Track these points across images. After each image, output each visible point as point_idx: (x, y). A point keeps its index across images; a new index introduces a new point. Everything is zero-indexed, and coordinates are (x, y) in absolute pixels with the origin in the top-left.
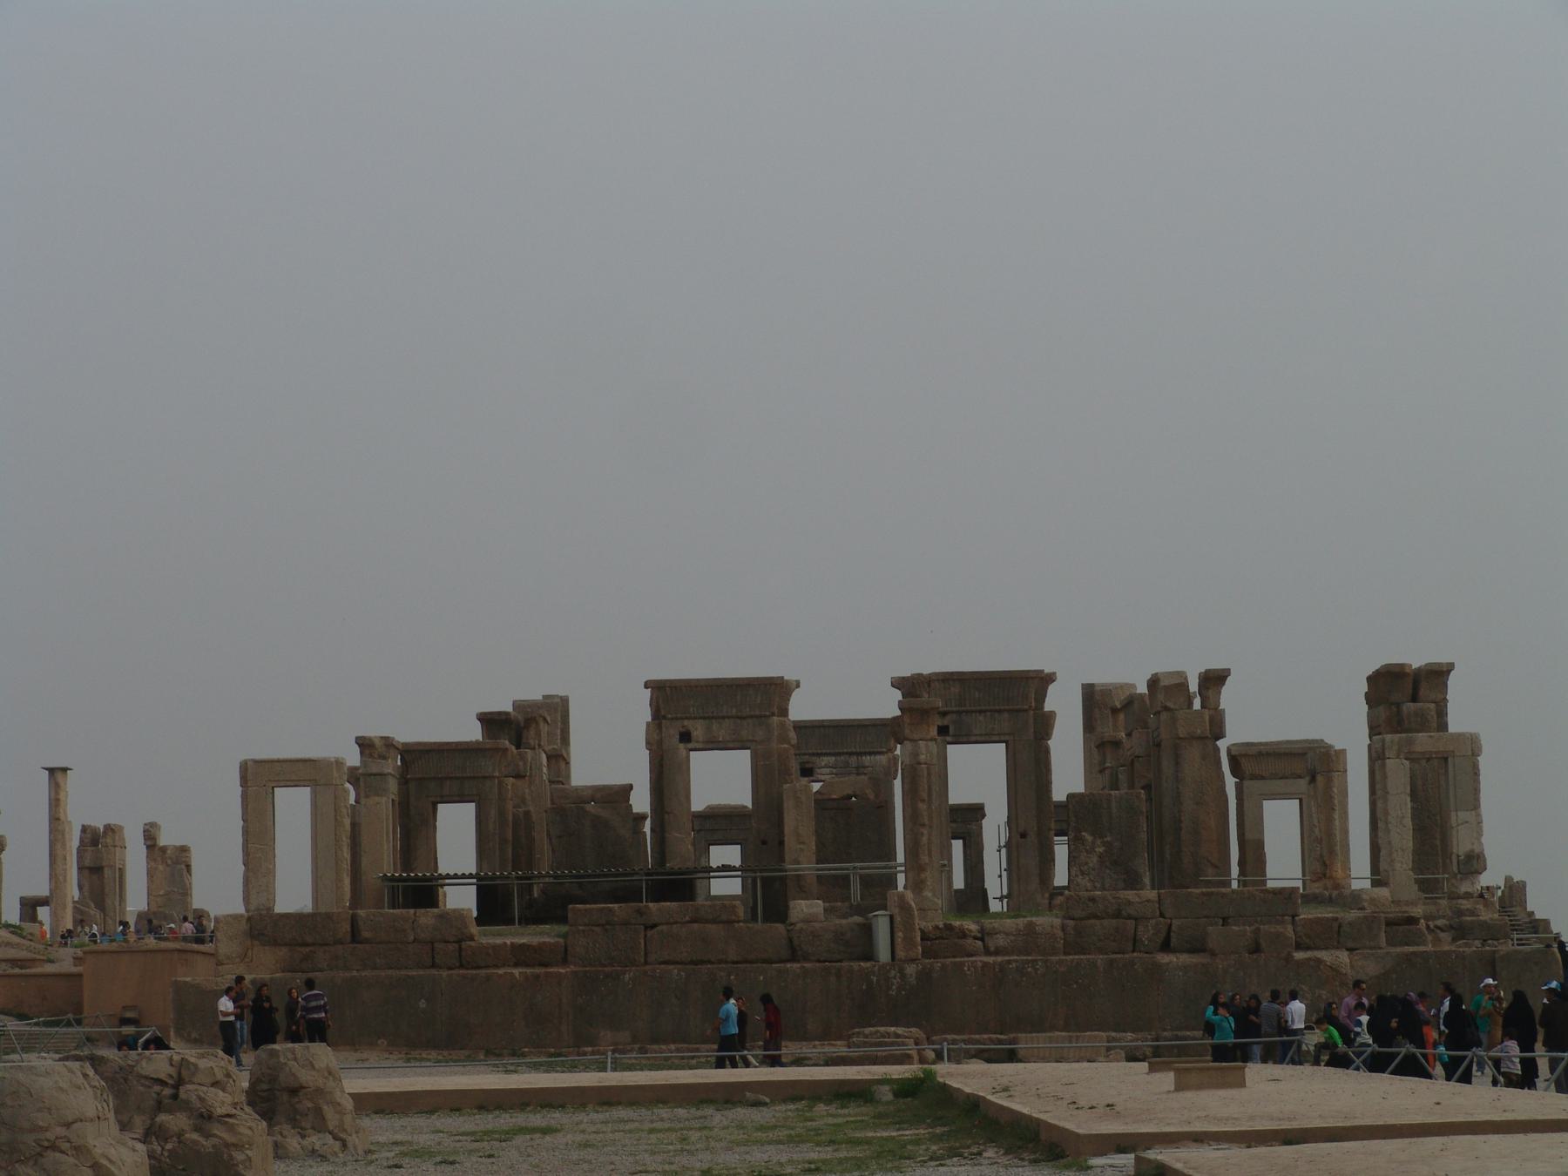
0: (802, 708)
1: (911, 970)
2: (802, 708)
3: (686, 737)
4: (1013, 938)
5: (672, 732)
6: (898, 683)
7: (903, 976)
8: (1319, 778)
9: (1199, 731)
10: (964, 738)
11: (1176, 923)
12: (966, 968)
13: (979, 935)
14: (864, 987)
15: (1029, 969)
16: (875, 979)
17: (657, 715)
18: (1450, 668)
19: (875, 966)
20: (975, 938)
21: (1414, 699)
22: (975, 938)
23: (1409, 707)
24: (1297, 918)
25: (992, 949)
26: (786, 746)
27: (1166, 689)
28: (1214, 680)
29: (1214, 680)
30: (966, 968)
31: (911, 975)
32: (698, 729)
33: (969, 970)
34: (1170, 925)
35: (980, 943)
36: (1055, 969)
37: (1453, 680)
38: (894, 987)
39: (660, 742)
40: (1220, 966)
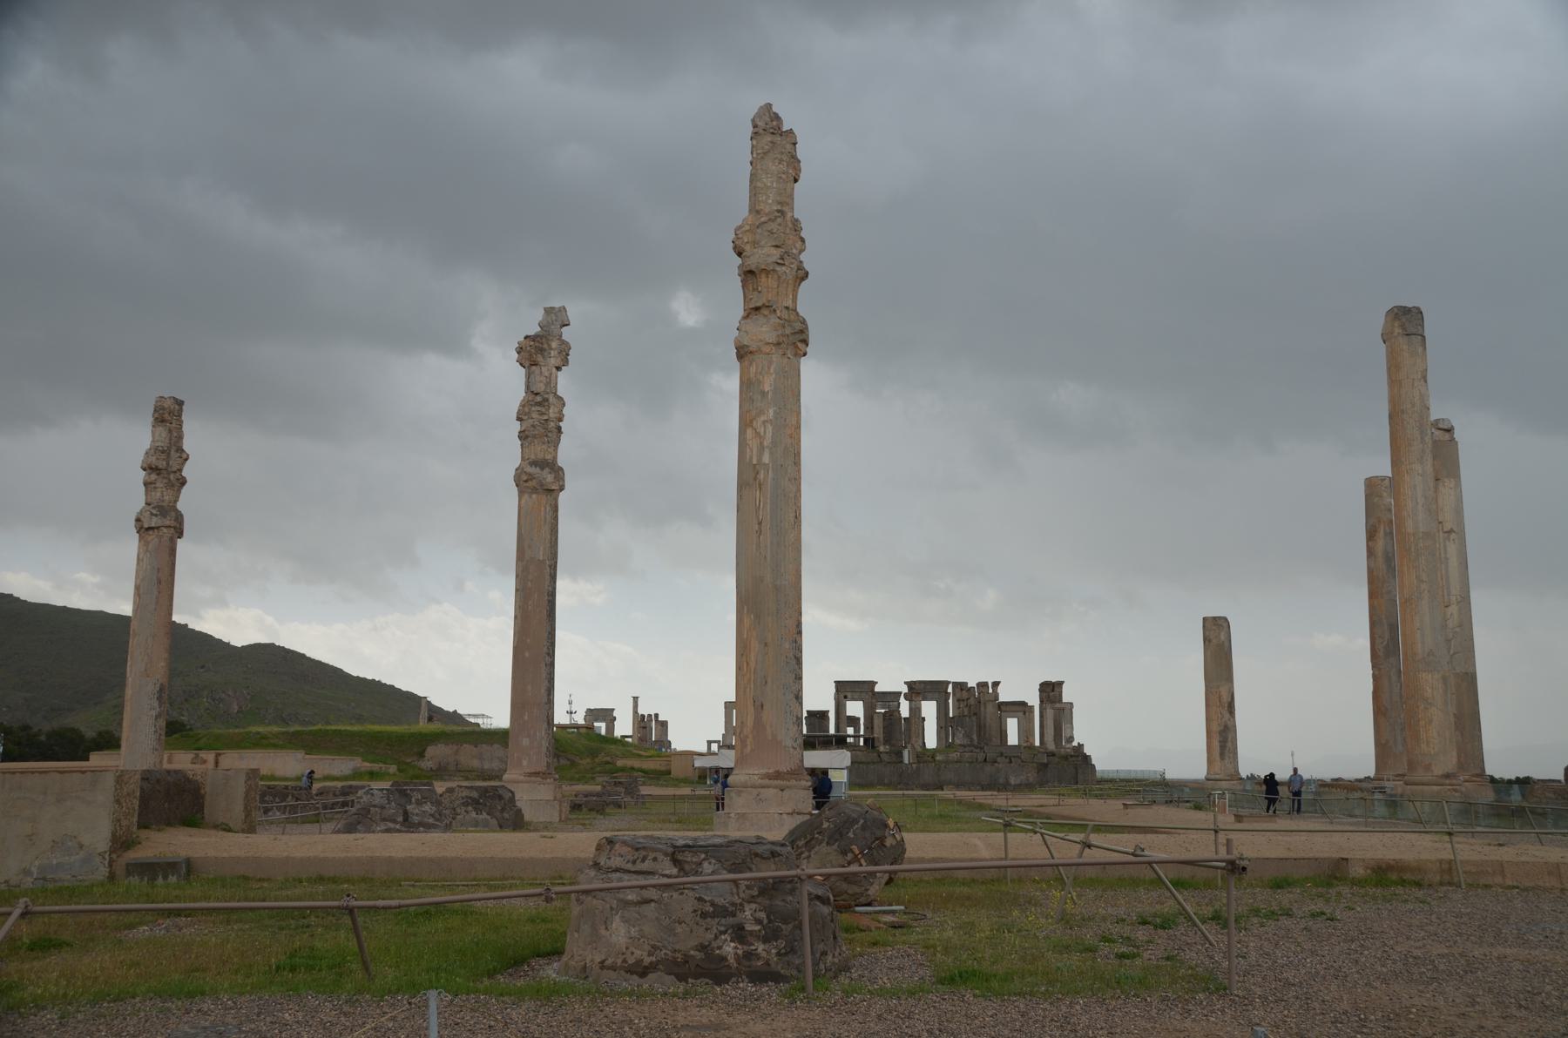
0: (877, 689)
1: (914, 766)
2: (877, 689)
3: (846, 697)
5: (842, 696)
6: (906, 683)
7: (912, 767)
8: (1027, 714)
10: (925, 699)
17: (837, 691)
18: (1063, 682)
21: (1053, 691)
23: (1051, 694)
27: (982, 685)
28: (996, 684)
29: (996, 684)
32: (849, 695)
37: (1064, 685)
39: (838, 698)
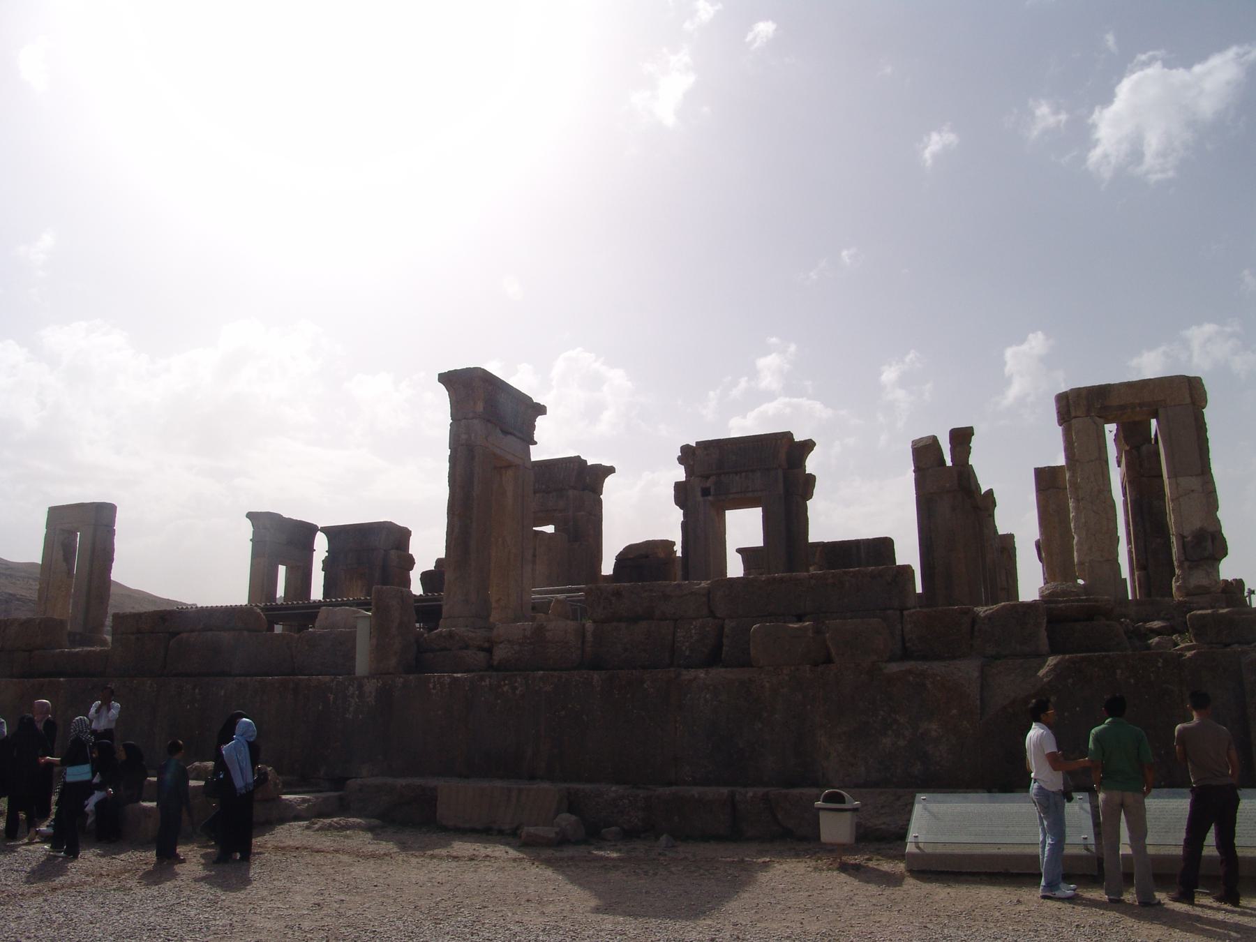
4: (517, 648)
9: (948, 485)
11: (729, 625)
12: (431, 686)
13: (486, 645)
14: (320, 708)
15: (505, 689)
16: (332, 697)
19: (333, 681)
20: (481, 649)
22: (481, 649)
24: (906, 612)
25: (495, 663)
26: (583, 513)
30: (431, 686)
31: (370, 692)
33: (434, 688)
34: (722, 628)
35: (482, 655)
36: (537, 688)
38: (351, 709)
40: (767, 685)
